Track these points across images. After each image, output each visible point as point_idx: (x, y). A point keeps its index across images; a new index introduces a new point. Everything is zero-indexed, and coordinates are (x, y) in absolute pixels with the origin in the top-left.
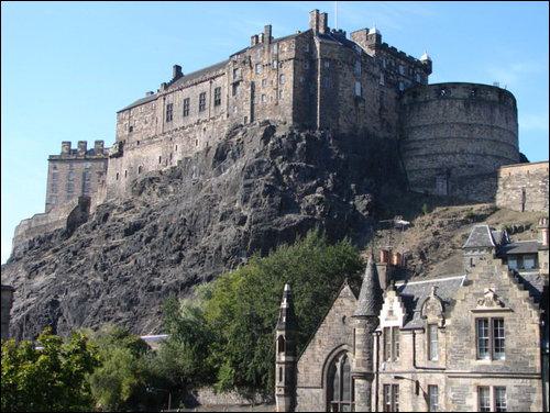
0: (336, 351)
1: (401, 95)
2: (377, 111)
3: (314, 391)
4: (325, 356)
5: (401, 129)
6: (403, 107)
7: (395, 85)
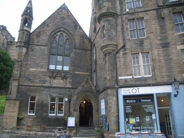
0: (57, 30)
1: (8, 42)
2: (2, 43)
3: (42, 47)
4: (50, 32)
5: (6, 49)
6: (8, 44)
7: (7, 39)
